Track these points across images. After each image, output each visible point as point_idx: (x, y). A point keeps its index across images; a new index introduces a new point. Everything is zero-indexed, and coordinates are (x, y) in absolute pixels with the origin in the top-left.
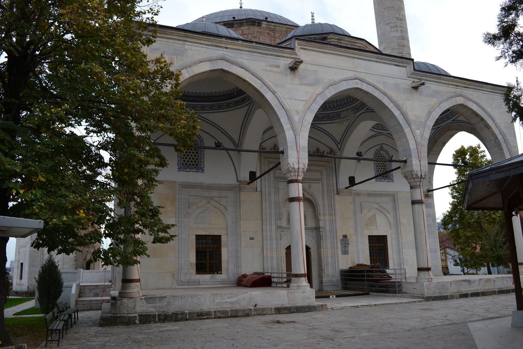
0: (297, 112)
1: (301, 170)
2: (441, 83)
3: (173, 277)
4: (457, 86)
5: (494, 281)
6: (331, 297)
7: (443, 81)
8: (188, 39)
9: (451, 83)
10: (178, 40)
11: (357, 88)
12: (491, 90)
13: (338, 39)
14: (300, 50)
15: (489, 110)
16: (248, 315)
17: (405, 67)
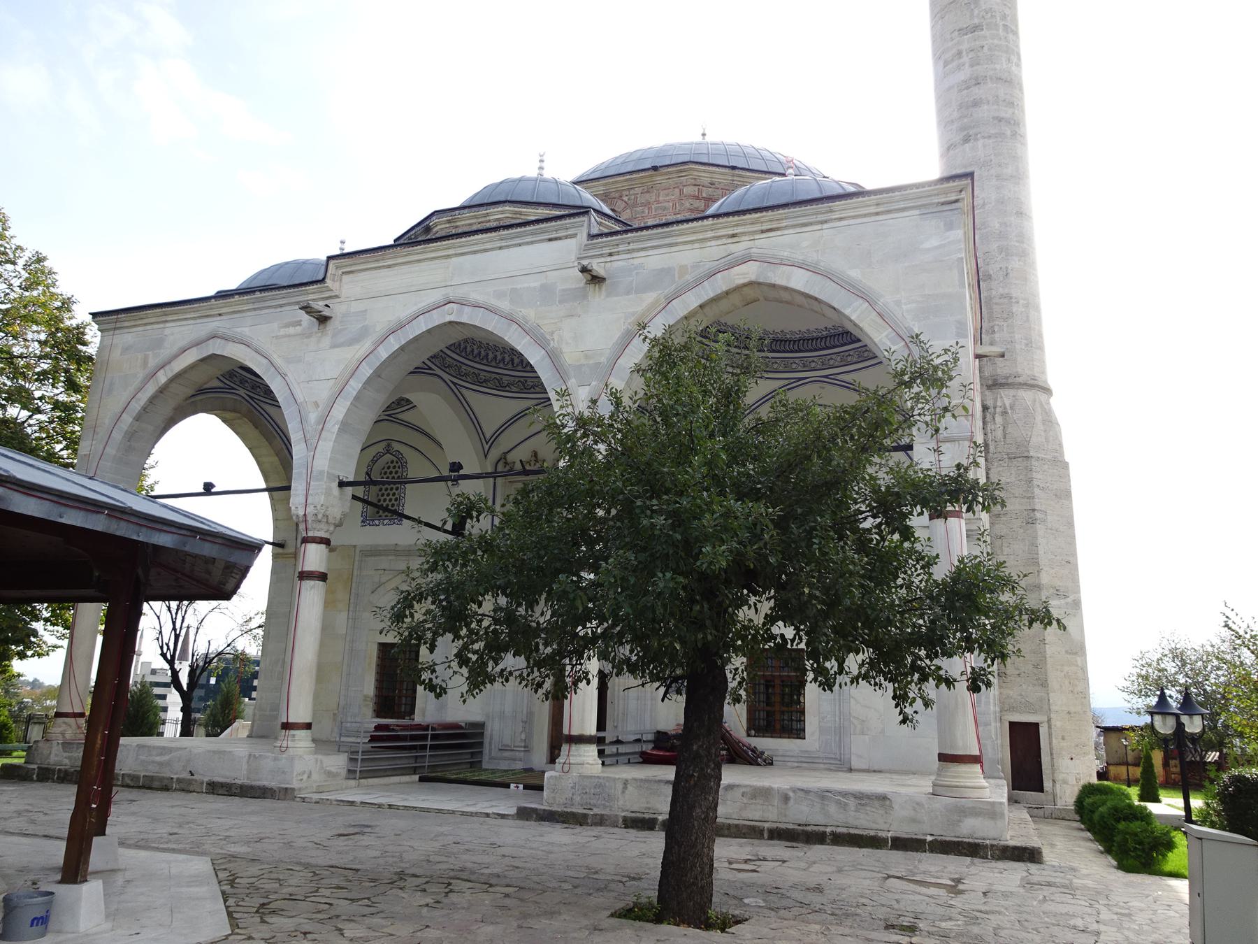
0: (316, 404)
1: (310, 519)
2: (677, 244)
3: (334, 720)
4: (734, 236)
5: (786, 798)
6: (512, 786)
7: (680, 239)
8: (169, 318)
9: (709, 234)
10: (158, 323)
11: (450, 322)
12: (873, 210)
13: (449, 222)
14: (345, 278)
15: (854, 274)
16: (166, 789)
17: (574, 236)
